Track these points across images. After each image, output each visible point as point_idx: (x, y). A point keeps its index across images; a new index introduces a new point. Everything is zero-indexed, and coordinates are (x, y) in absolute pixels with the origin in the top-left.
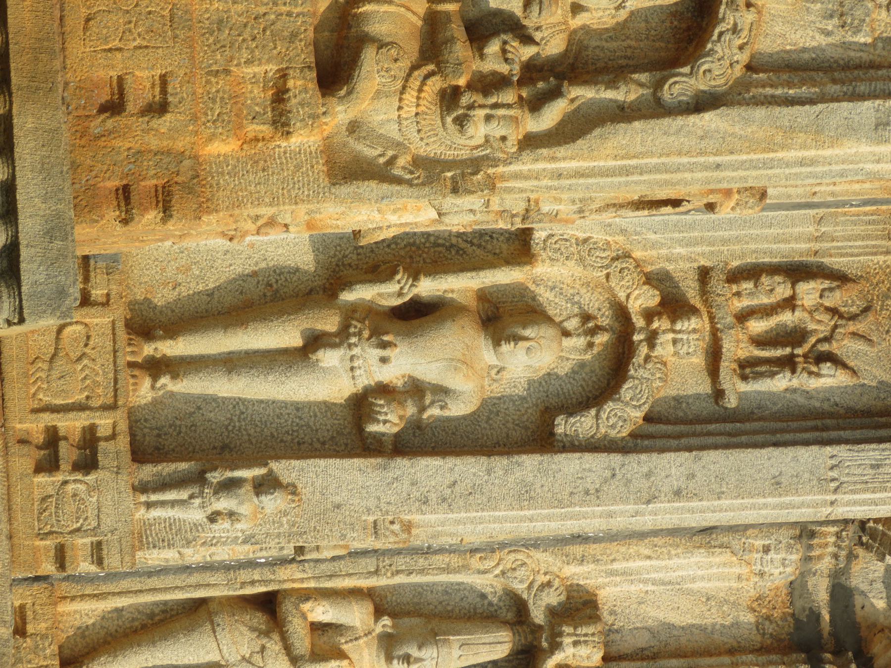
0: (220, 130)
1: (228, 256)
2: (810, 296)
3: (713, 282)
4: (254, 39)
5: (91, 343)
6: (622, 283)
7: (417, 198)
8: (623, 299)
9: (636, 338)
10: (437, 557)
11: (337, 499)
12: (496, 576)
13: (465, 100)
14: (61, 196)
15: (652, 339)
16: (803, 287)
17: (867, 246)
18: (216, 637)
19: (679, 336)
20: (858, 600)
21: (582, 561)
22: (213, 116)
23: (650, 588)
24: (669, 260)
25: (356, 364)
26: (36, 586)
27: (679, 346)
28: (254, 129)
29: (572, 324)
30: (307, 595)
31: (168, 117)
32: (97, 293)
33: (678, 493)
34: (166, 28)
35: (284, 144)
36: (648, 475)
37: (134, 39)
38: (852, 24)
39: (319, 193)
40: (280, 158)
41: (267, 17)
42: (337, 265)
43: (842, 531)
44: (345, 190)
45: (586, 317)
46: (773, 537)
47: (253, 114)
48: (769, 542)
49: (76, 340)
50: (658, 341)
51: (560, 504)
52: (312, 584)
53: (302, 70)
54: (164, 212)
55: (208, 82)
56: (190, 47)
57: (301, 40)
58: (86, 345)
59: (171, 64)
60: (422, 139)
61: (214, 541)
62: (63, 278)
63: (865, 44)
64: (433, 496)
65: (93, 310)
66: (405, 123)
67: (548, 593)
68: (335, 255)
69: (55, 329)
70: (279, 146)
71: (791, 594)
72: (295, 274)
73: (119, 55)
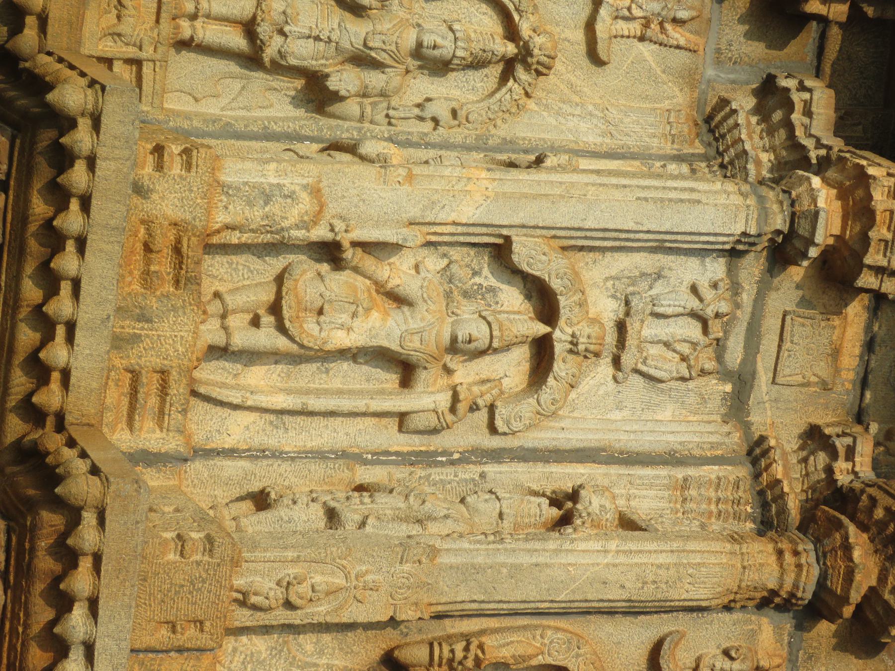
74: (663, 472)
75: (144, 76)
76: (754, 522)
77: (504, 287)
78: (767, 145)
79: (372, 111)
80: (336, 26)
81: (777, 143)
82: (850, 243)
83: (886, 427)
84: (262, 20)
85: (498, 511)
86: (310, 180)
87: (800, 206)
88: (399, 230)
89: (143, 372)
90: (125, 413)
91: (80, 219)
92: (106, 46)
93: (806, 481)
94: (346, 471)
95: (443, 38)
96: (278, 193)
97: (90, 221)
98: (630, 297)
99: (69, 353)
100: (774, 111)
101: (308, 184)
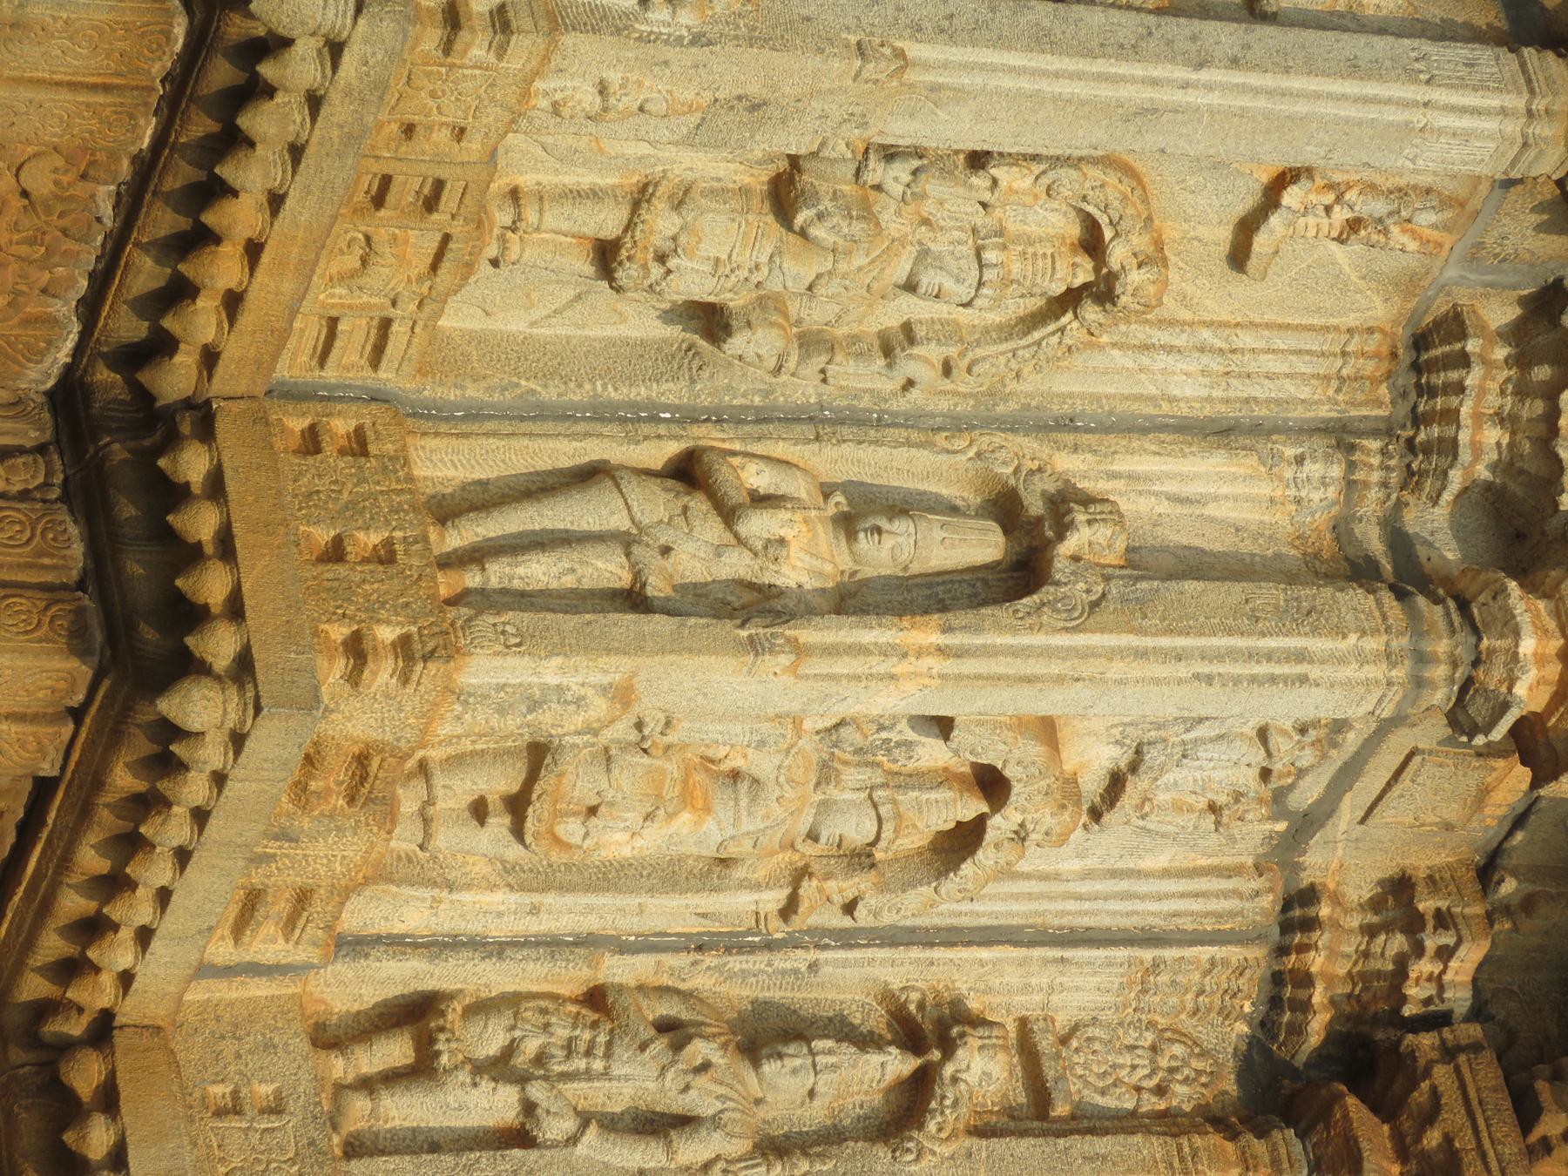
10: (892, 430)
11: (805, 12)
12: (970, 459)
18: (620, 491)
20: (1422, 552)
21: (1076, 449)
23: (1164, 507)
26: (374, 406)
30: (734, 453)
33: (1234, 62)
36: (1194, 38)
43: (1387, 445)
46: (1306, 444)
48: (1301, 450)
51: (1091, 54)
52: (737, 446)
61: (652, 37)
64: (926, 24)
67: (1041, 479)
71: (1337, 539)
74: (1121, 953)
75: (392, 338)
76: (1250, 1024)
77: (923, 739)
78: (1507, 409)
79: (799, 364)
80: (764, 259)
81: (1525, 414)
82: (1551, 734)
83: (1529, 888)
84: (629, 258)
85: (809, 1087)
86: (618, 677)
87: (1486, 672)
88: (756, 726)
89: (270, 890)
90: (231, 920)
91: (187, 830)
92: (333, 296)
93: (1360, 964)
94: (585, 968)
95: (958, 280)
96: (555, 698)
97: (202, 839)
98: (1145, 749)
99: (136, 958)
100: (1540, 363)
101: (611, 685)
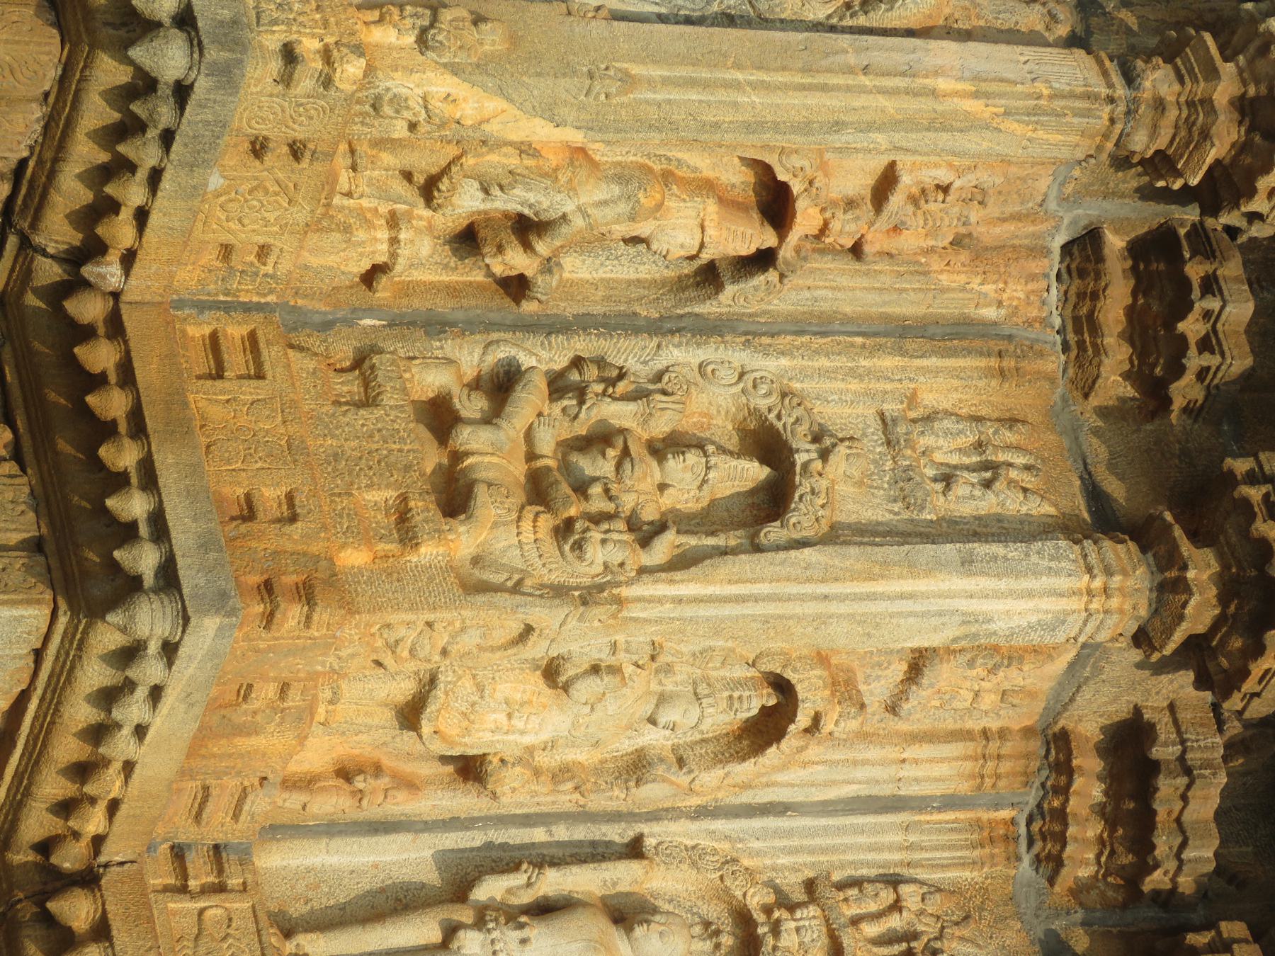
0: (351, 540)
1: (354, 875)
2: (913, 899)
3: (820, 888)
4: (370, 468)
5: (234, 925)
6: (737, 883)
7: (550, 607)
8: (740, 898)
9: (761, 930)
13: (579, 526)
14: (210, 516)
15: (776, 929)
16: (905, 889)
17: (954, 858)
19: (801, 923)
22: (342, 528)
24: (774, 869)
25: (497, 948)
27: (803, 932)
28: (382, 547)
29: (697, 930)
31: (299, 524)
32: (234, 882)
34: (284, 454)
35: (415, 559)
37: (256, 462)
38: (915, 503)
39: (455, 601)
40: (412, 571)
41: (379, 452)
42: (461, 882)
44: (480, 599)
45: (707, 924)
47: (380, 535)
49: (218, 922)
50: (783, 928)
53: (420, 494)
54: (308, 604)
55: (332, 501)
56: (311, 469)
57: (415, 471)
58: (229, 926)
59: (294, 483)
60: (544, 565)
62: (224, 583)
63: (931, 521)
65: (231, 896)
66: (526, 548)
68: (457, 873)
69: (196, 912)
70: (410, 561)
72: (421, 889)
73: (243, 474)
